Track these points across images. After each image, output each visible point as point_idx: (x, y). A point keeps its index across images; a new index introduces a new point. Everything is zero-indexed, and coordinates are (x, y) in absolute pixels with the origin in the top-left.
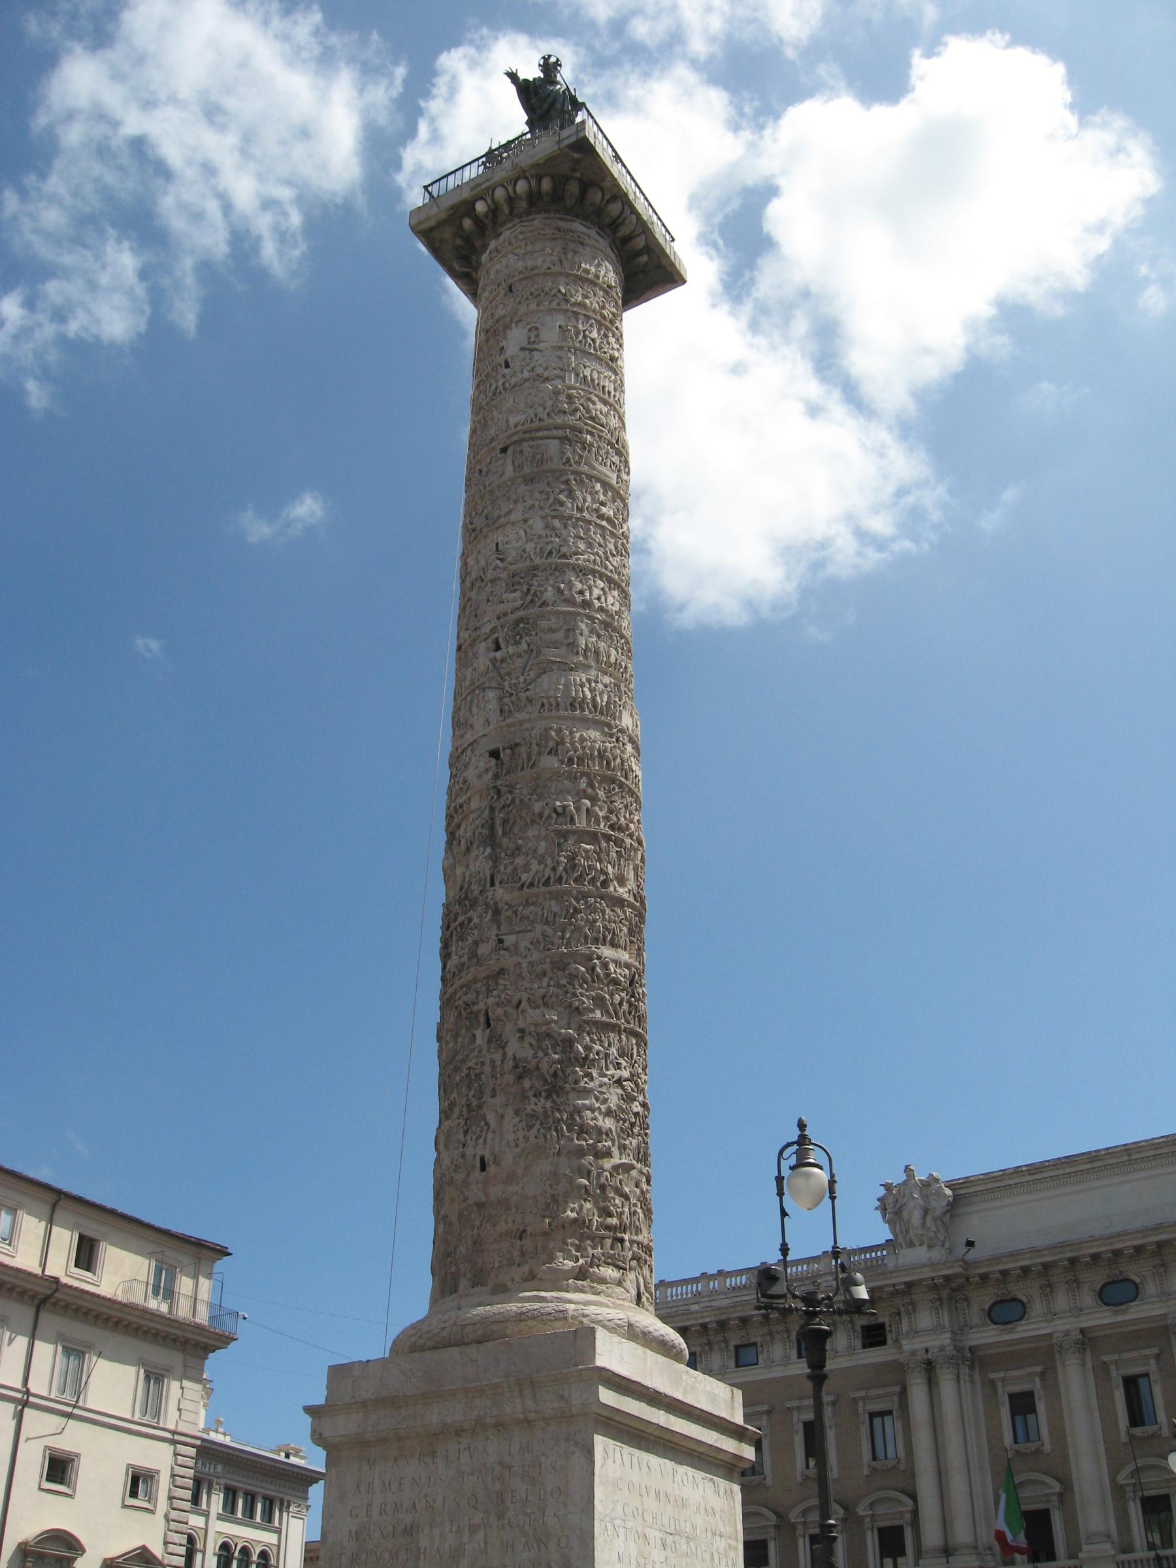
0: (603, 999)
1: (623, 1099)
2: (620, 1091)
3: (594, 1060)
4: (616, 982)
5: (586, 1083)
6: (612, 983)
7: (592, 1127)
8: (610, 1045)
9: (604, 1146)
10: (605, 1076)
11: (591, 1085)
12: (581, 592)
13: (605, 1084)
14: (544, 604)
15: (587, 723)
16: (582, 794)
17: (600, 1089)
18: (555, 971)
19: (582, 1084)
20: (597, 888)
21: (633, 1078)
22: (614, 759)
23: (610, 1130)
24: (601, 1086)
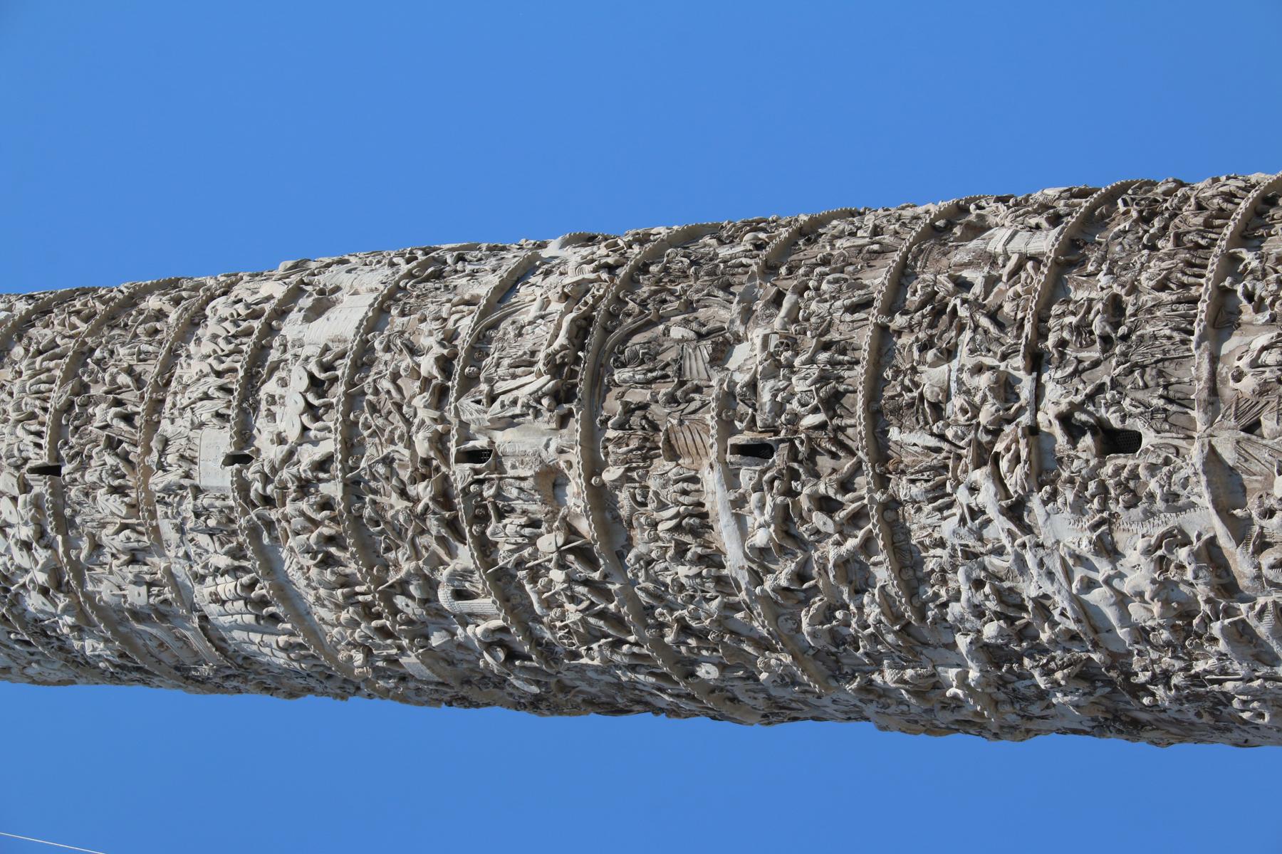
0: (844, 564)
1: (1053, 496)
2: (1035, 502)
3: (1000, 594)
4: (785, 520)
5: (1063, 614)
6: (793, 532)
7: (1166, 603)
8: (941, 544)
9: (1196, 577)
10: (1021, 561)
11: (1061, 601)
12: (44, 591)
13: (1041, 564)
14: (122, 655)
15: (284, 590)
16: (433, 605)
17: (1060, 575)
18: (846, 669)
19: (1073, 626)
20: (605, 576)
21: (985, 456)
22: (316, 524)
23: (1148, 551)
24: (1050, 575)
